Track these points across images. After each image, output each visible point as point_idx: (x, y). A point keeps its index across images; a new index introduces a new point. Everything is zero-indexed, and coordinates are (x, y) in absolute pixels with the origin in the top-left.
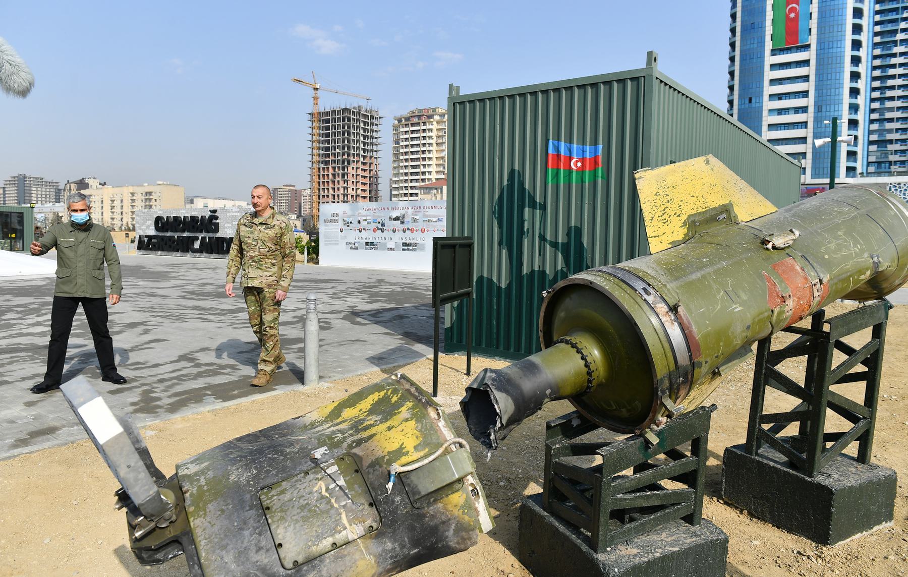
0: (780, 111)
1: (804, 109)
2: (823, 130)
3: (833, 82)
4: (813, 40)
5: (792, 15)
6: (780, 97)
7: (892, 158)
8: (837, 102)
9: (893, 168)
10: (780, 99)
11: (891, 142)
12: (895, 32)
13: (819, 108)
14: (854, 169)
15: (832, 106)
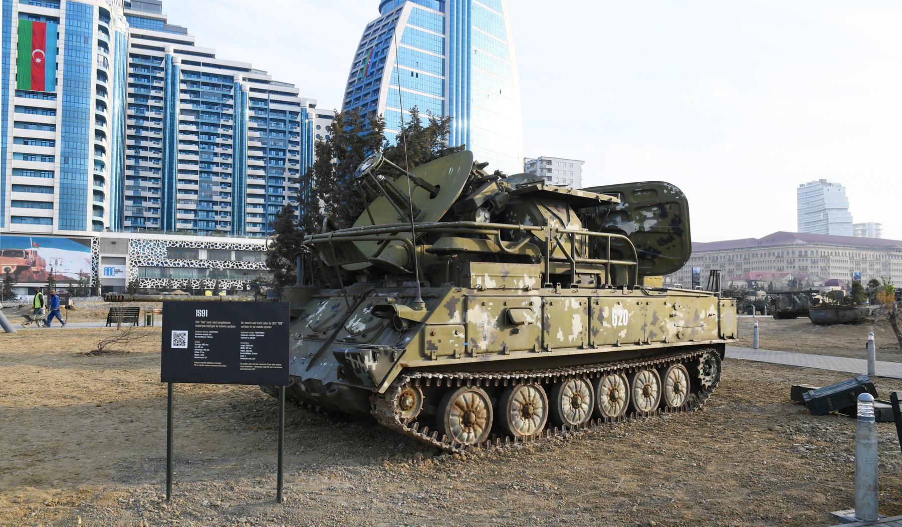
0: (26, 156)
1: (51, 158)
2: (70, 182)
3: (79, 136)
4: (59, 90)
5: (38, 60)
6: (26, 141)
7: (147, 214)
8: (82, 156)
9: (149, 224)
10: (26, 143)
11: (145, 199)
12: (146, 97)
13: (66, 159)
14: (101, 223)
15: (78, 160)
